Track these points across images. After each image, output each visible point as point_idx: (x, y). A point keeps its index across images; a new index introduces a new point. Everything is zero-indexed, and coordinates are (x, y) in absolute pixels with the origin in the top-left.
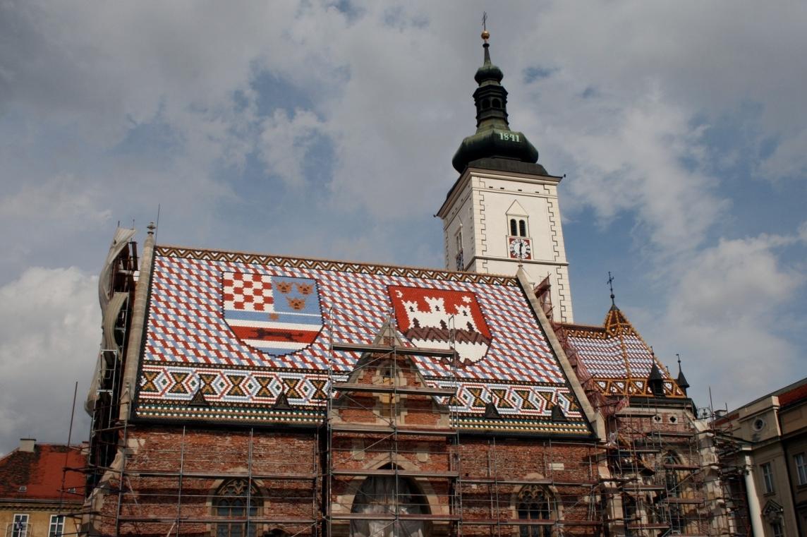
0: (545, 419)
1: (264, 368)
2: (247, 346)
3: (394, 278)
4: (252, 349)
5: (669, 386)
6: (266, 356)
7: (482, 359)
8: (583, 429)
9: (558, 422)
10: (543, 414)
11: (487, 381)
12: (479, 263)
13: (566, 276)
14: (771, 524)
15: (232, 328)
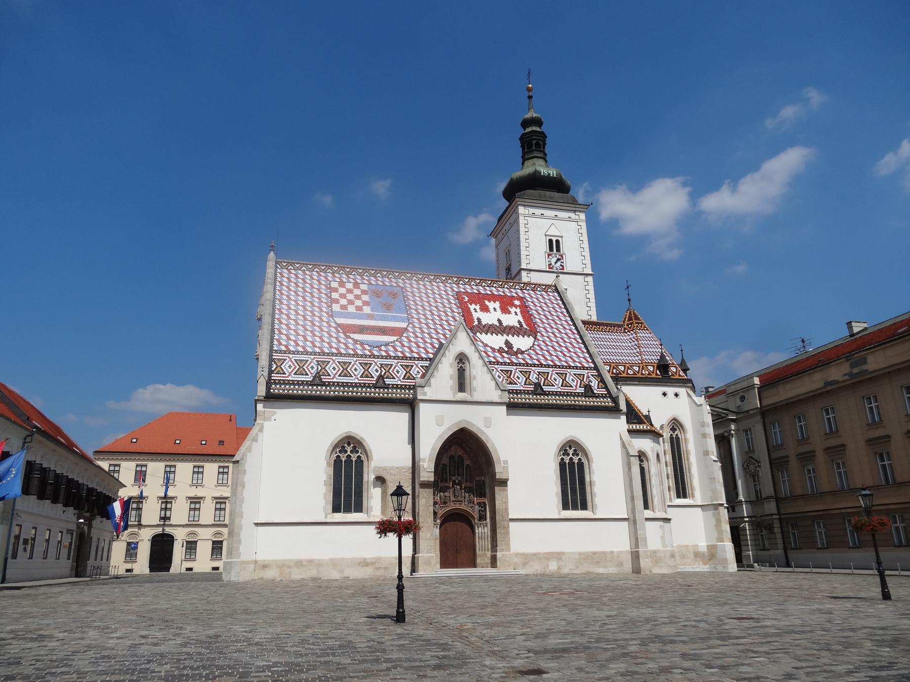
0: (578, 395)
1: (366, 356)
2: (352, 339)
3: (461, 286)
4: (355, 341)
7: (531, 349)
8: (608, 403)
9: (589, 397)
10: (578, 391)
11: (534, 365)
12: (524, 274)
13: (591, 284)
14: (750, 475)
15: (339, 325)
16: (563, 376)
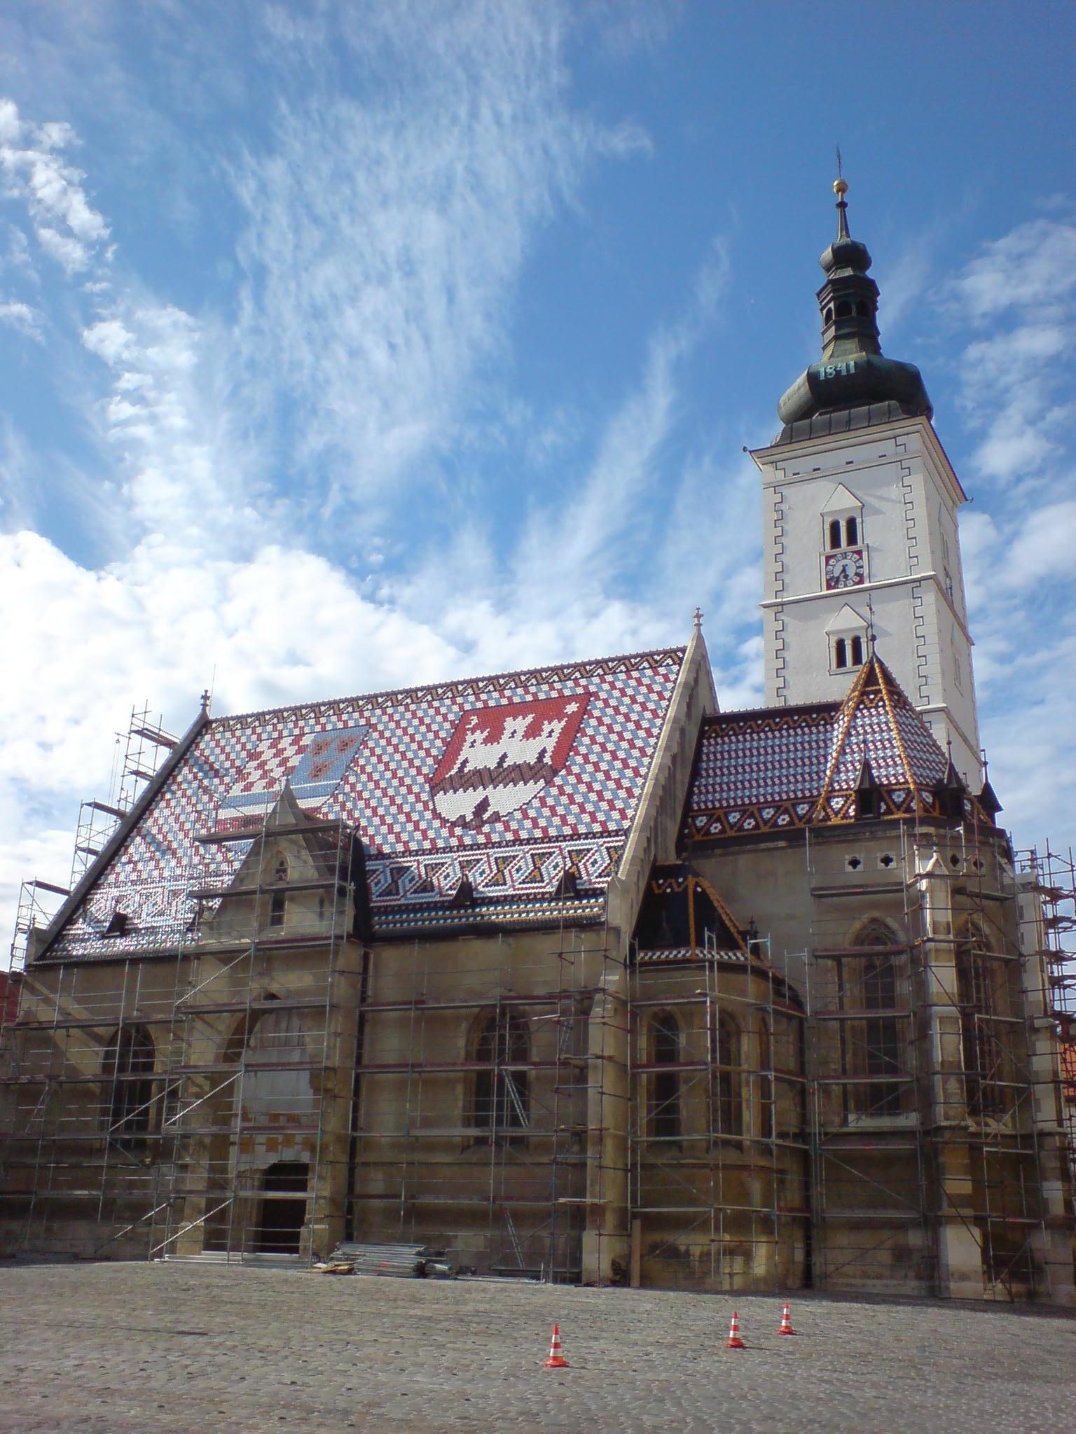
10: (549, 889)
16: (538, 858)
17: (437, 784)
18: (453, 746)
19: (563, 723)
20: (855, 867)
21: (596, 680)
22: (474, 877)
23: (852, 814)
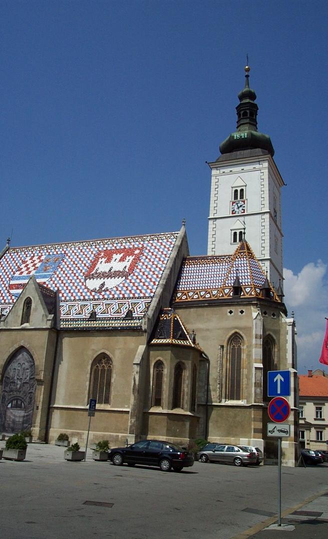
5: (248, 290)
6: (13, 297)
17: (89, 276)
18: (94, 264)
19: (133, 257)
20: (231, 314)
21: (146, 242)
22: (97, 310)
23: (231, 294)
